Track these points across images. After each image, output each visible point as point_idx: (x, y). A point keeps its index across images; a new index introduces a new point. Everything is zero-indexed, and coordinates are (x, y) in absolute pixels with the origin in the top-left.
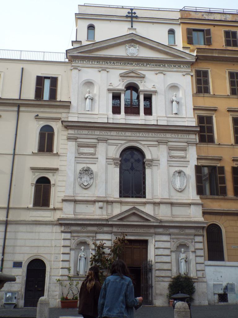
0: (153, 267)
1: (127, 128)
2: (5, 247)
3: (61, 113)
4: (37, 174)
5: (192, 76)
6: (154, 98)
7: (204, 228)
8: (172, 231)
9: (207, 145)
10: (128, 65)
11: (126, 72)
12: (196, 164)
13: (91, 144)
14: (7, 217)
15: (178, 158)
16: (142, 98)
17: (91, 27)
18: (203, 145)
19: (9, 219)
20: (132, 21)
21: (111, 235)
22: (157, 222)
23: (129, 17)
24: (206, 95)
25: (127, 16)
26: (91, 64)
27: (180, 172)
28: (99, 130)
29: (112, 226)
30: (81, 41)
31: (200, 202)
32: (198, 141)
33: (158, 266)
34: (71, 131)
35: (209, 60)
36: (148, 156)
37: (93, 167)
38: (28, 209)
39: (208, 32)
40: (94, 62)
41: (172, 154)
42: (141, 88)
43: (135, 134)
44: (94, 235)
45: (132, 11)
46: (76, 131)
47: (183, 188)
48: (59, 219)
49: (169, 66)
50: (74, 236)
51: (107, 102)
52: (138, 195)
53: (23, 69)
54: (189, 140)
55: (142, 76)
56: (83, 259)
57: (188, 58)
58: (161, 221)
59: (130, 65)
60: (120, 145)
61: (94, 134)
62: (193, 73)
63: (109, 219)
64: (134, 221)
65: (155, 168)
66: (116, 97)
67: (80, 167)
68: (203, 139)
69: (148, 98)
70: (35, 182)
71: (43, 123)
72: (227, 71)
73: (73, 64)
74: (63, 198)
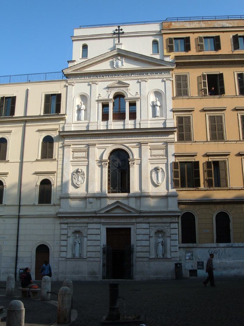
0: (135, 250)
1: (113, 133)
2: (19, 235)
6: (138, 104)
7: (180, 216)
8: (151, 220)
9: (185, 142)
11: (113, 83)
14: (19, 213)
15: (158, 156)
16: (127, 104)
17: (85, 47)
18: (181, 143)
19: (21, 214)
20: (119, 37)
21: (100, 225)
22: (137, 213)
24: (186, 97)
25: (114, 34)
28: (90, 136)
29: (100, 217)
33: (139, 249)
35: (191, 65)
36: (131, 157)
38: (34, 205)
39: (187, 40)
44: (86, 225)
45: (119, 28)
48: (57, 214)
50: (70, 227)
51: (96, 111)
53: (28, 90)
56: (78, 245)
58: (140, 212)
62: (174, 79)
63: (97, 212)
64: (118, 212)
66: (105, 106)
68: (181, 138)
69: (133, 104)
71: (44, 134)
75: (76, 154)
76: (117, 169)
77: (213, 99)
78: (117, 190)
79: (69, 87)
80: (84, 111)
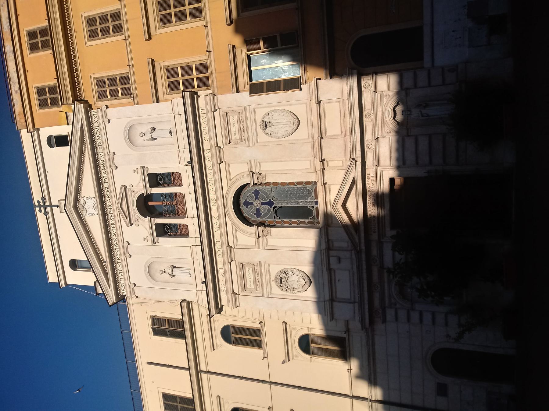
3: (200, 314)
4: (295, 353)
5: (107, 107)
10: (112, 212)
12: (248, 93)
13: (240, 272)
15: (242, 127)
16: (155, 190)
20: (51, 206)
23: (45, 210)
25: (46, 214)
26: (123, 269)
27: (266, 125)
30: (94, 282)
31: (313, 83)
32: (209, 92)
34: (224, 300)
37: (275, 270)
40: (119, 264)
41: (238, 138)
42: (142, 191)
43: (214, 201)
46: (222, 294)
47: (291, 118)
49: (100, 147)
52: (313, 194)
53: (149, 363)
54: (209, 108)
55: (123, 191)
57: (81, 117)
59: (112, 210)
60: (234, 227)
61: (223, 267)
62: (103, 104)
65: (265, 168)
67: (276, 290)
70: (308, 356)
71: (219, 340)
72: (89, 43)
73: (129, 295)
74: (329, 319)
75: (250, 284)
76: (272, 208)
77: (129, 22)
78: (313, 207)
79: (137, 292)
80: (174, 269)
